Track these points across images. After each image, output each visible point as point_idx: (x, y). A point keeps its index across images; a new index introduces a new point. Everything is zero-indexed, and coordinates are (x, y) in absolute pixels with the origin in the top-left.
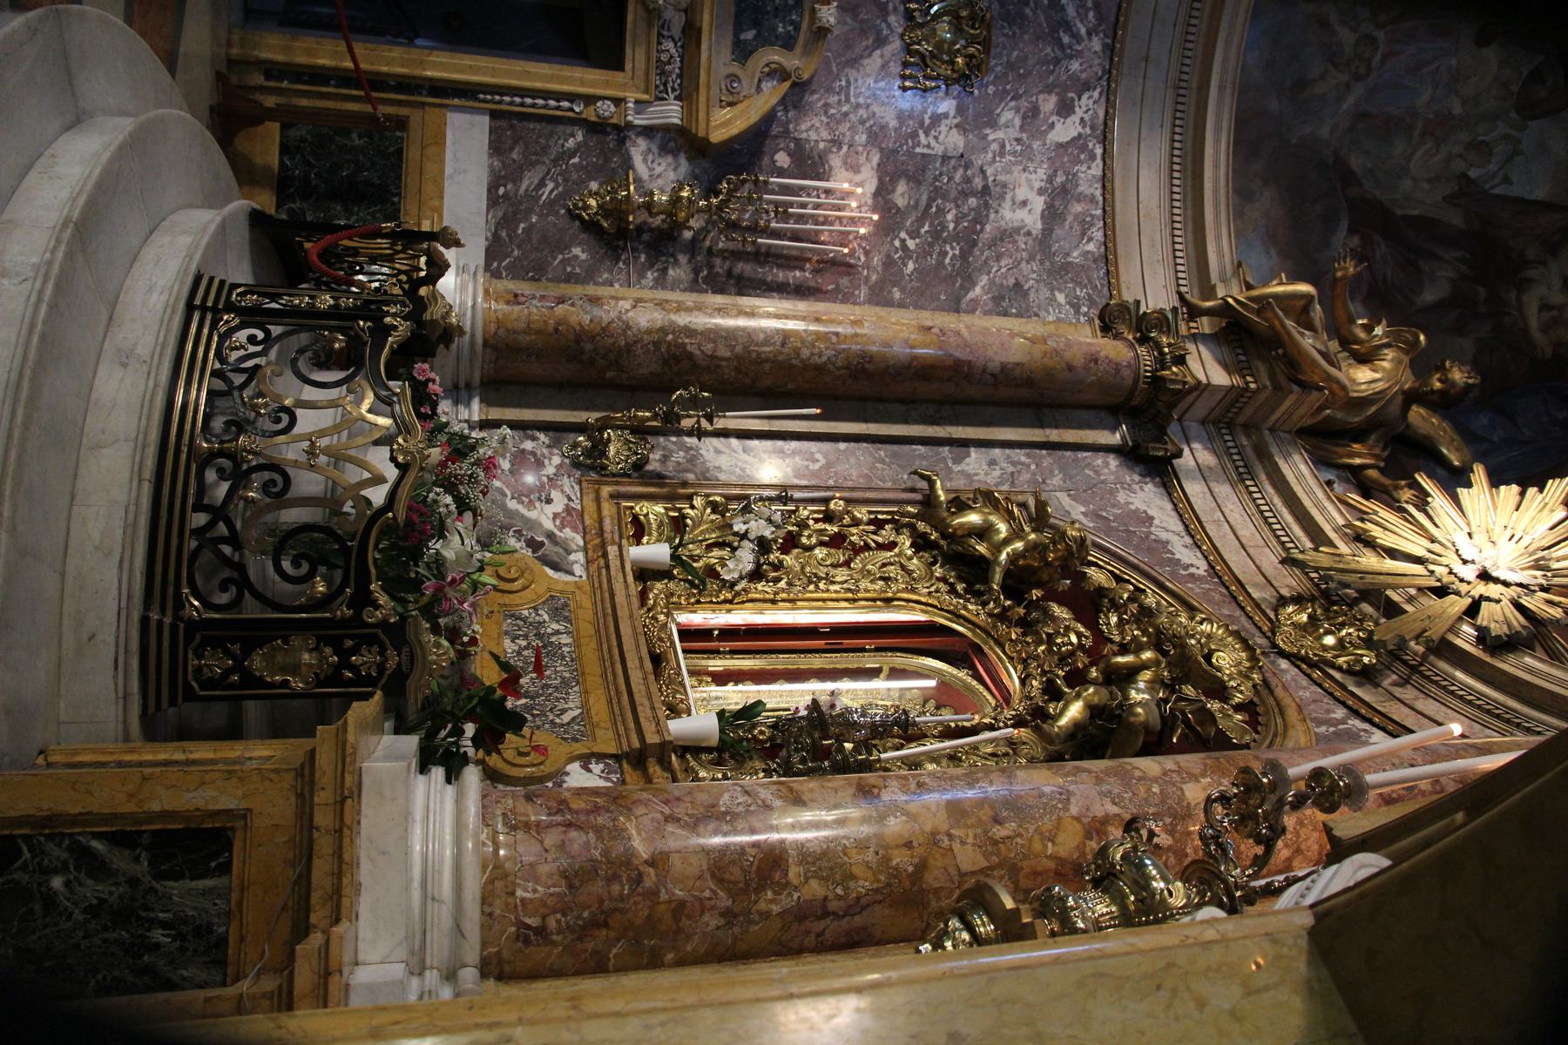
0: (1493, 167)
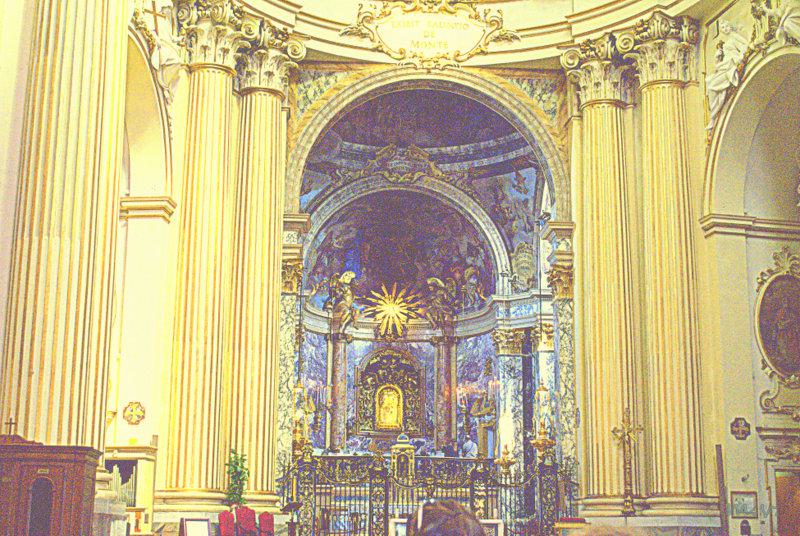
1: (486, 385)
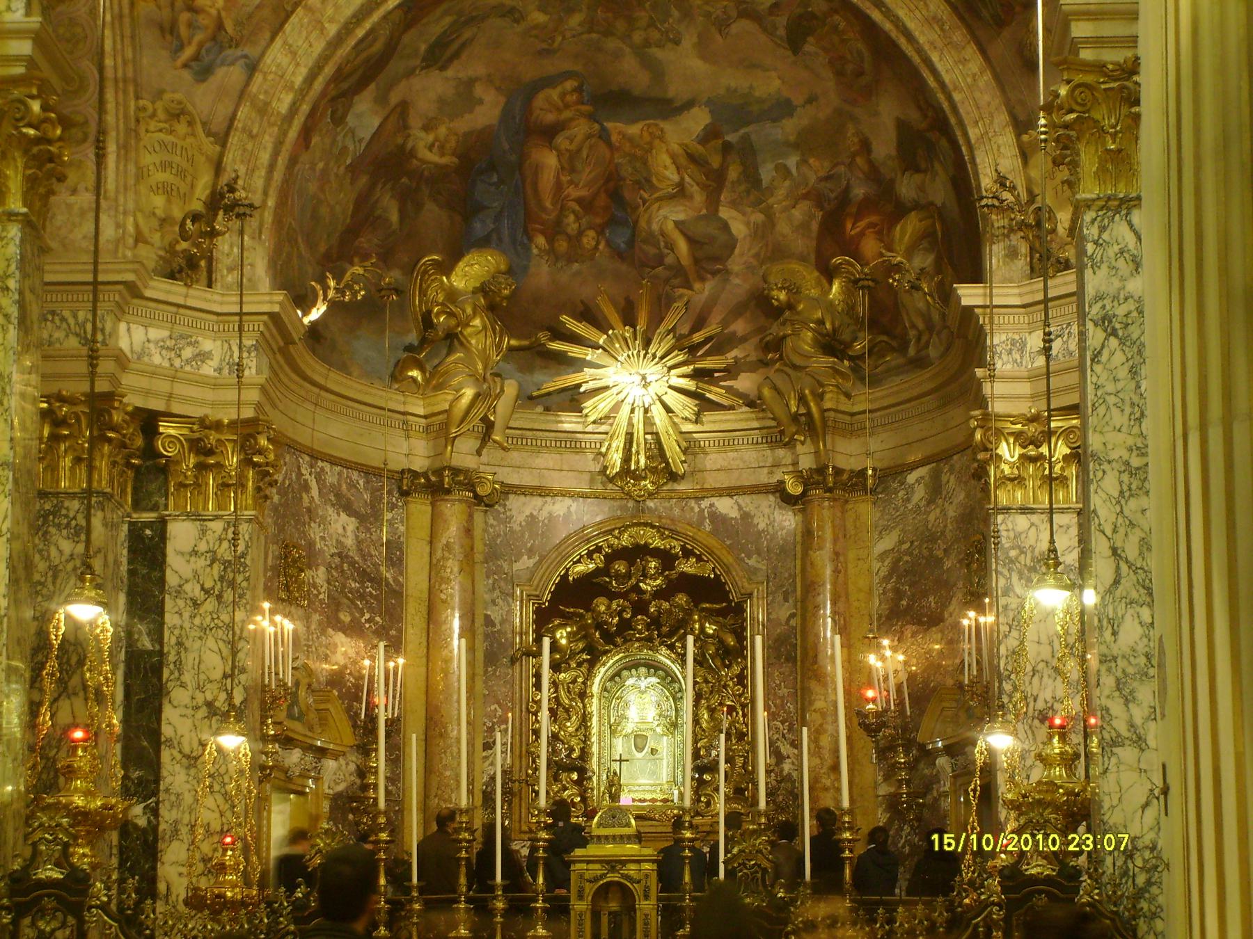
0: (351, 148)
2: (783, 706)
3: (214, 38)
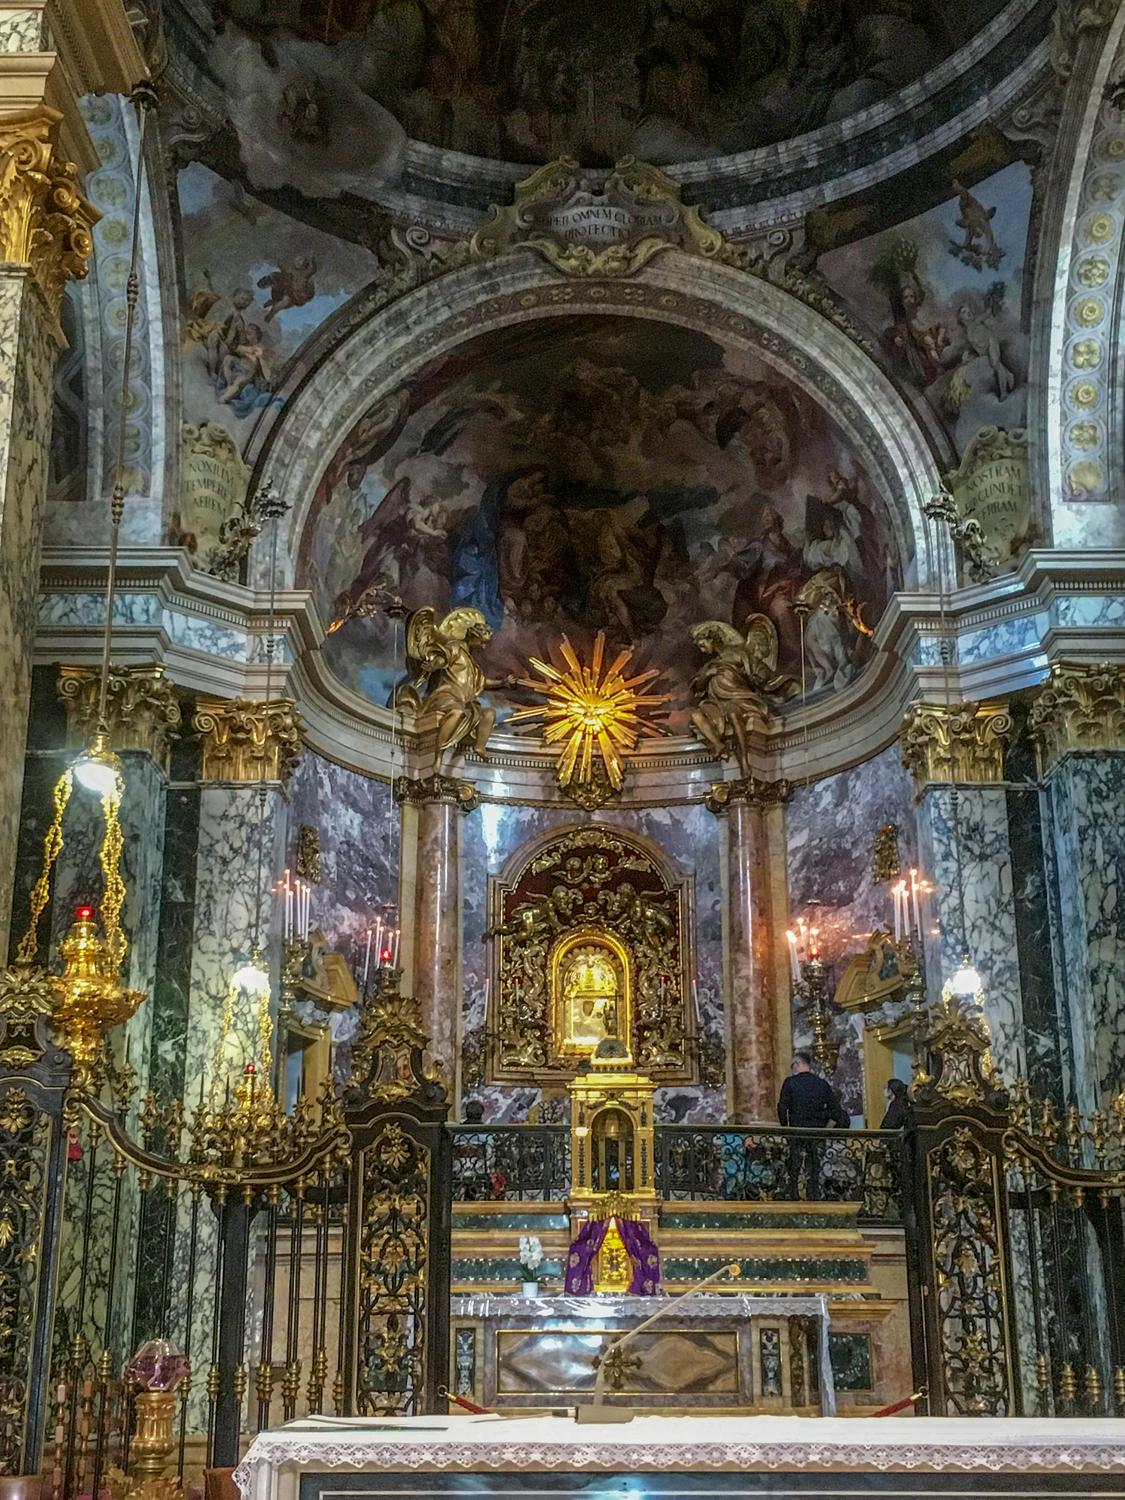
1: (885, 910)
2: (710, 975)
3: (253, 382)
